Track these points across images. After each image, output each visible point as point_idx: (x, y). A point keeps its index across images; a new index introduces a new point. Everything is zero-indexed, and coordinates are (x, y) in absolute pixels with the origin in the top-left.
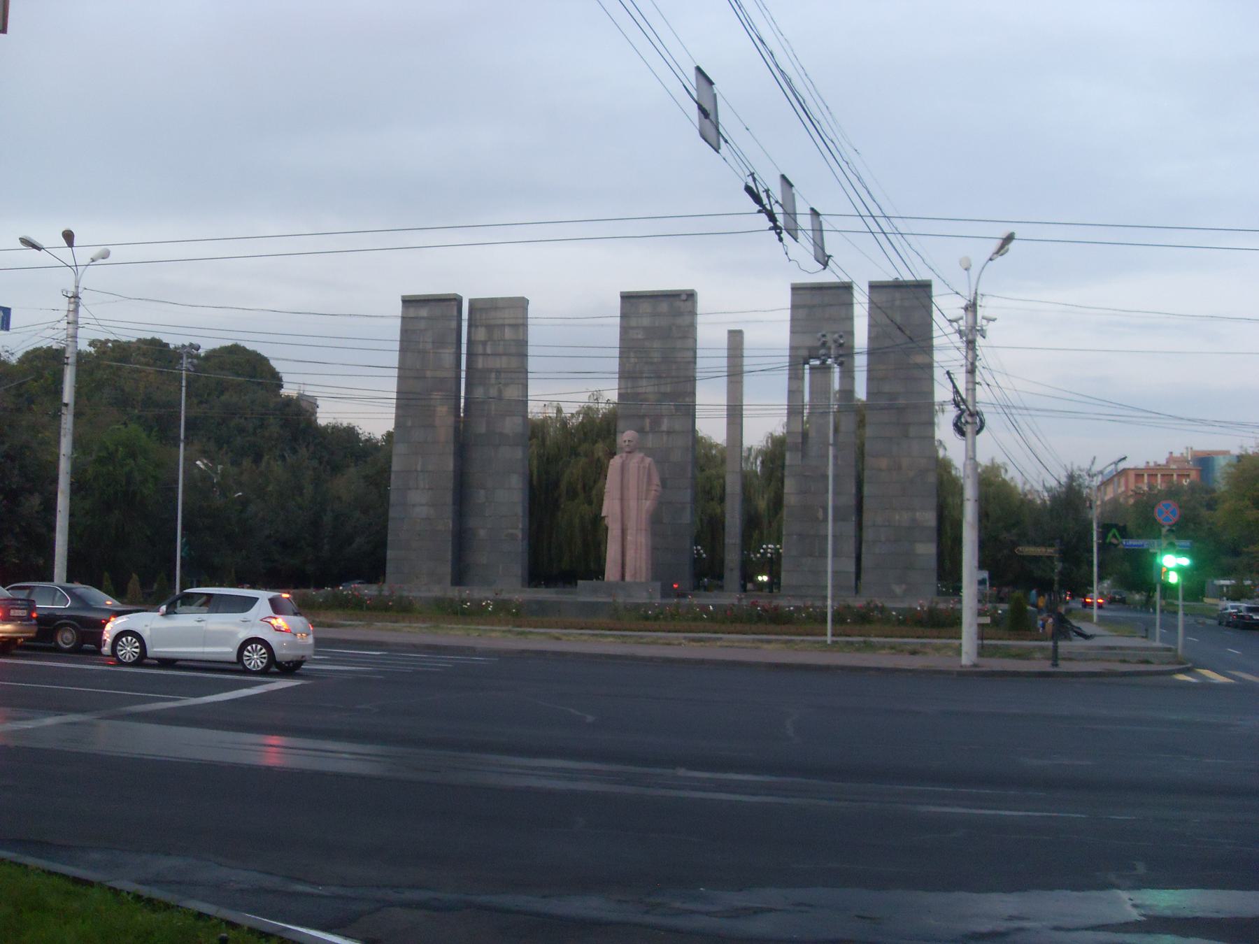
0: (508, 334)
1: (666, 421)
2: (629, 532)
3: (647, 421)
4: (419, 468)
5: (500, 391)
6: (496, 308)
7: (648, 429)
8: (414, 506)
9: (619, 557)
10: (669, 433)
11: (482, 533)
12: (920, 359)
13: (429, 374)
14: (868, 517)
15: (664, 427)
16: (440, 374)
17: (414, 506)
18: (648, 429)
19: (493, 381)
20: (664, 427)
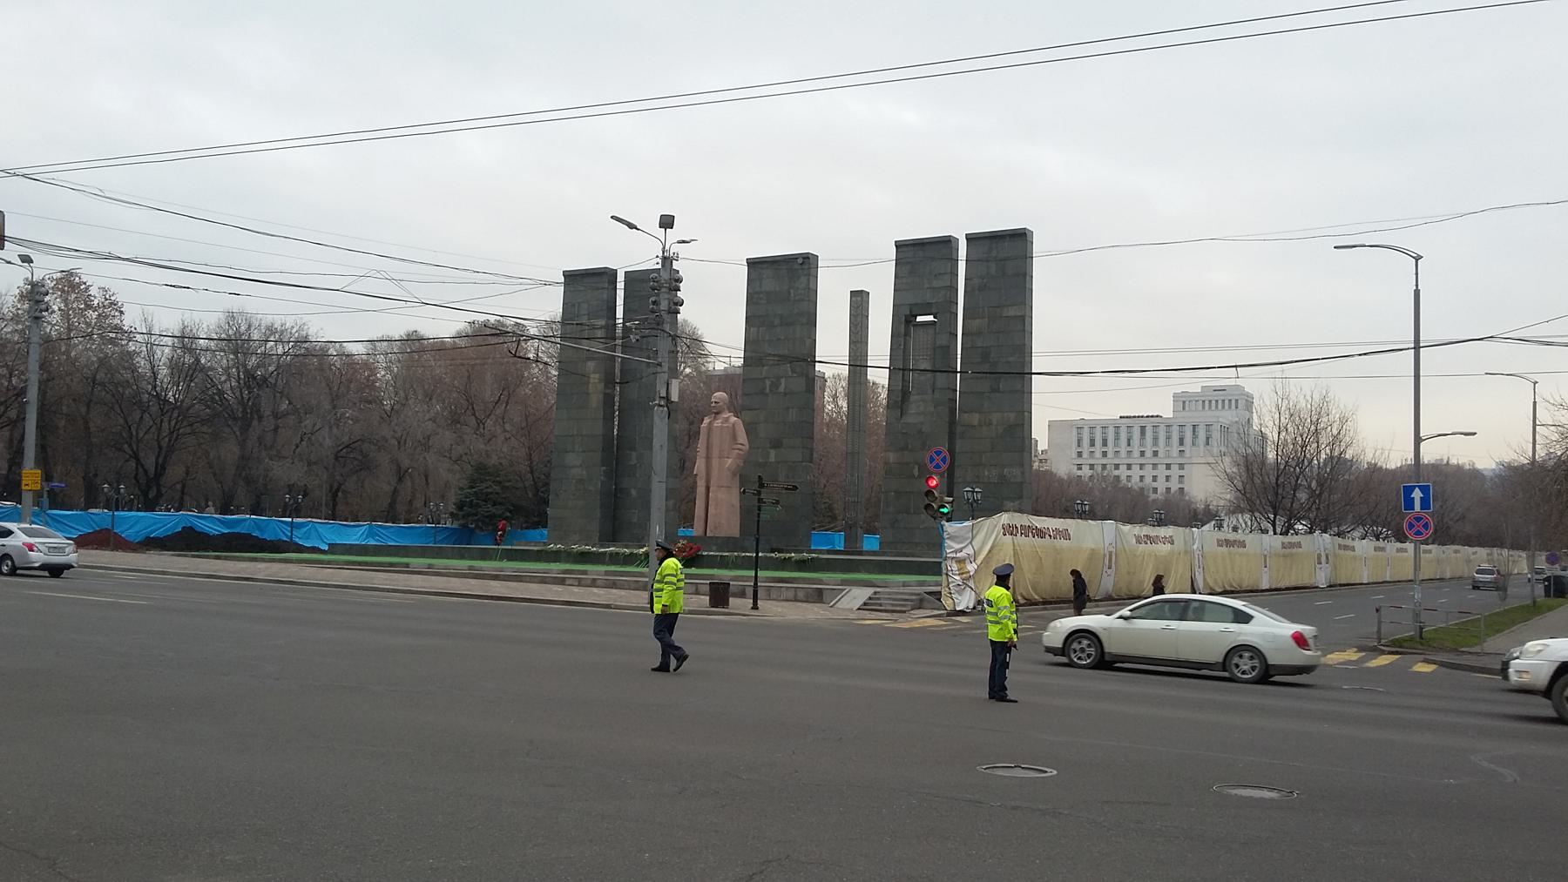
3: (768, 383)
11: (634, 492)
12: (1012, 312)
15: (782, 389)
20: (782, 389)
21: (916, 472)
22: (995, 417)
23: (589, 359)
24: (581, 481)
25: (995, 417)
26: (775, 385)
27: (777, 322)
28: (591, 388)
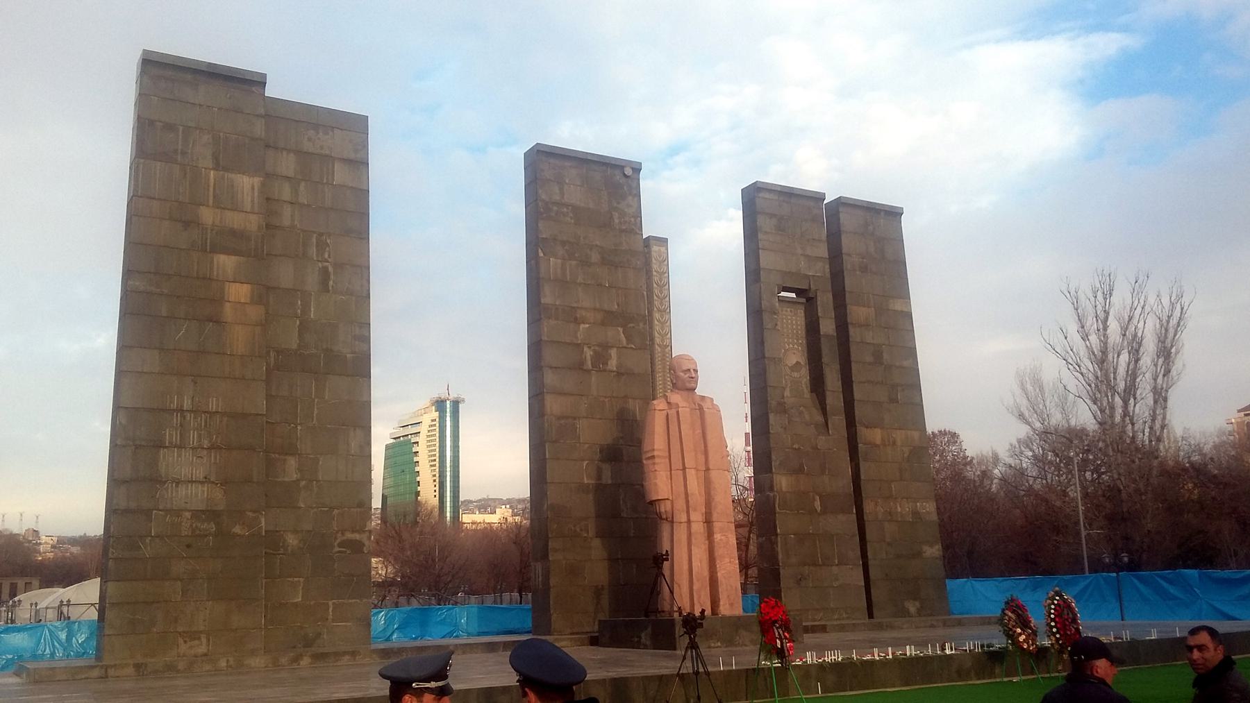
0: (341, 175)
1: (613, 352)
2: (717, 526)
4: (187, 404)
5: (325, 274)
6: (316, 127)
7: (589, 365)
8: (178, 482)
9: (706, 573)
10: (619, 374)
11: (292, 540)
13: (208, 215)
14: (868, 507)
16: (234, 220)
17: (178, 482)
18: (589, 365)
19: (313, 251)
20: (613, 364)
21: (817, 505)
22: (899, 436)
23: (215, 250)
24: (211, 514)
25: (899, 436)
26: (600, 359)
27: (595, 257)
28: (228, 312)
